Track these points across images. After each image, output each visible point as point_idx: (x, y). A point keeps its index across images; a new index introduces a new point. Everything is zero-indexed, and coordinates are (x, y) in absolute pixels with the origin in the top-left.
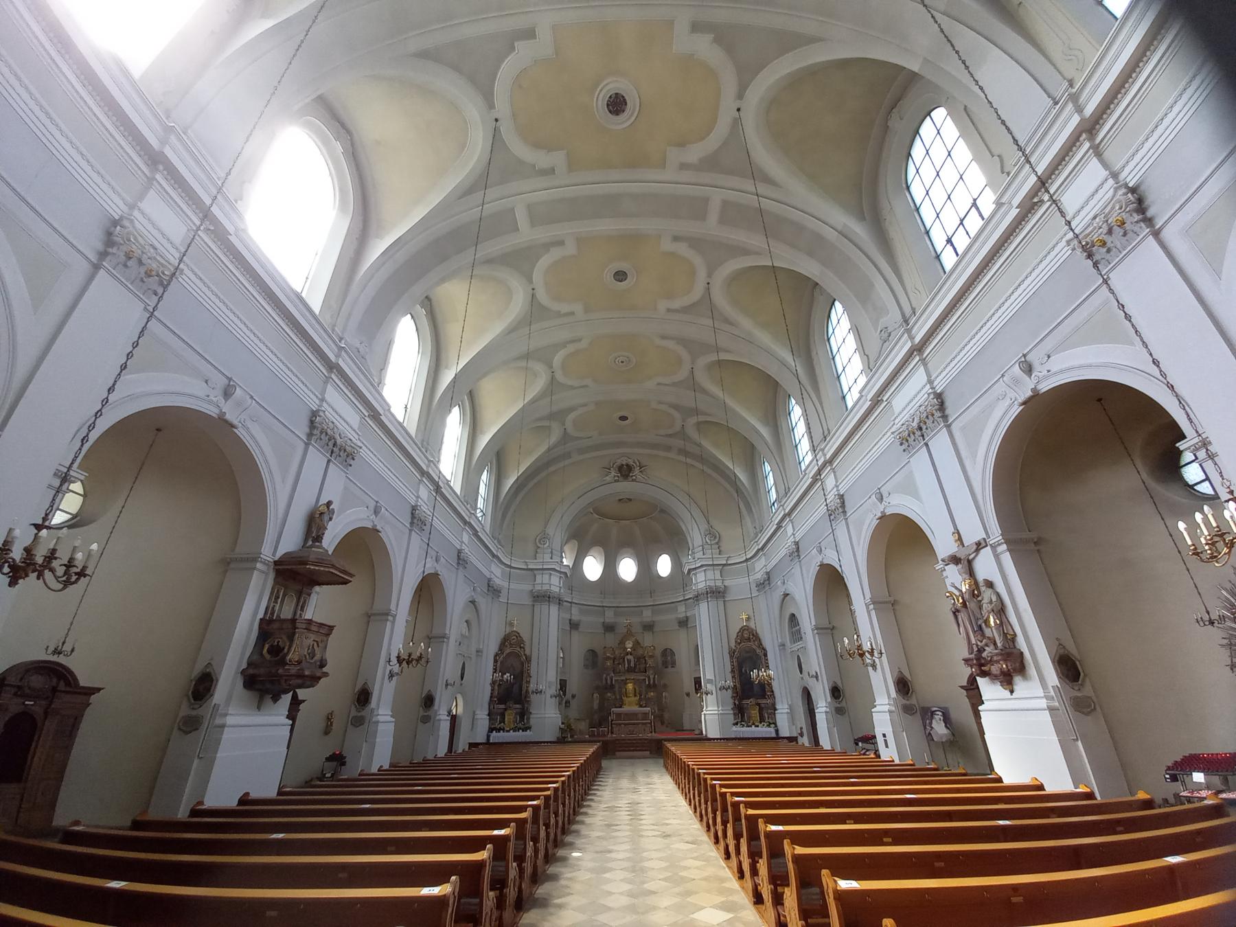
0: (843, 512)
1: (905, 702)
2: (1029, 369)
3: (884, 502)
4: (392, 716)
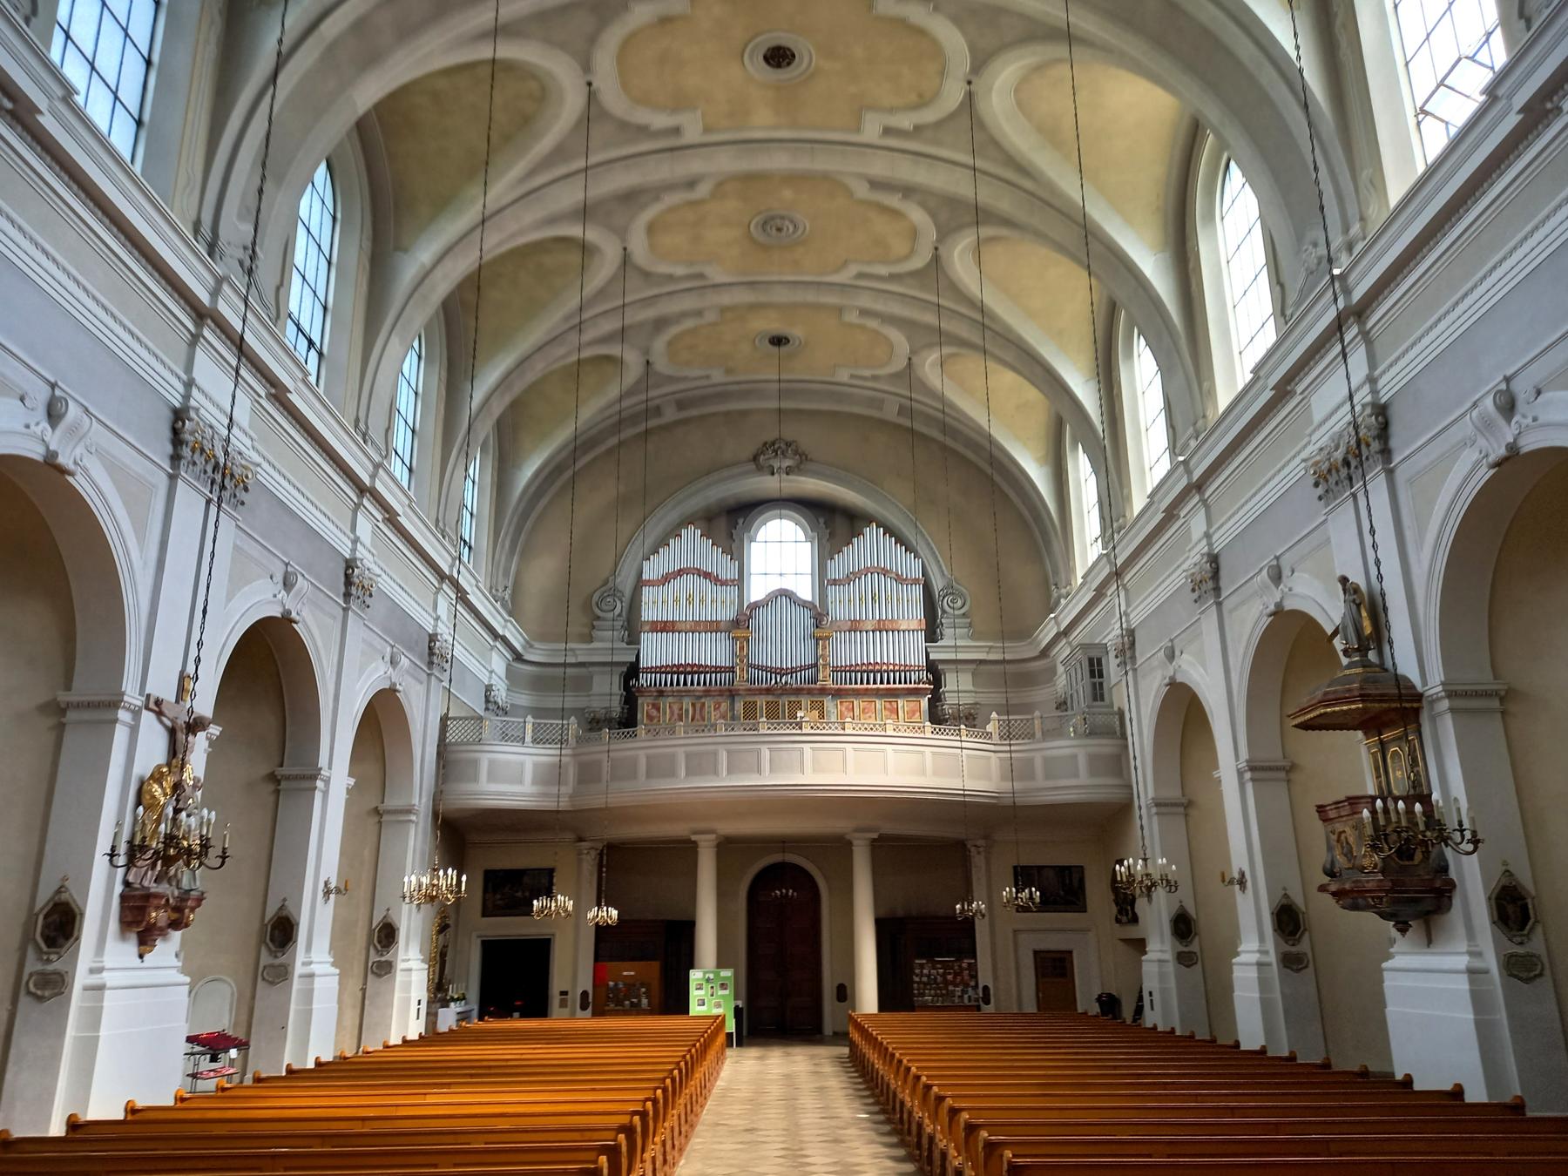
0: (1214, 589)
1: (1288, 948)
2: (1508, 406)
3: (1281, 586)
4: (334, 964)
